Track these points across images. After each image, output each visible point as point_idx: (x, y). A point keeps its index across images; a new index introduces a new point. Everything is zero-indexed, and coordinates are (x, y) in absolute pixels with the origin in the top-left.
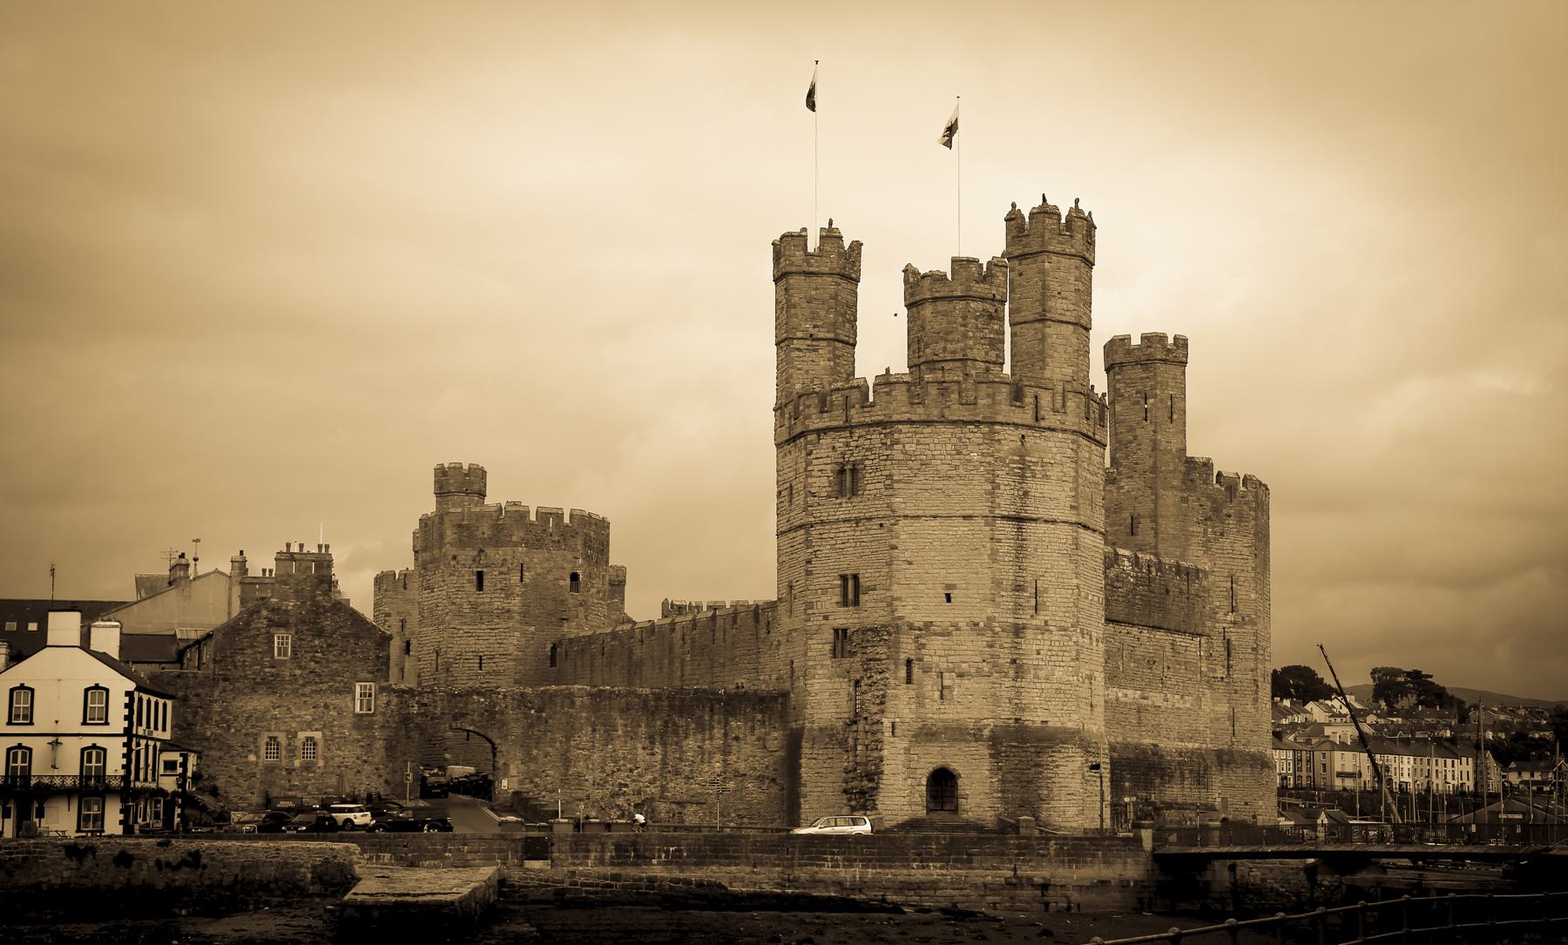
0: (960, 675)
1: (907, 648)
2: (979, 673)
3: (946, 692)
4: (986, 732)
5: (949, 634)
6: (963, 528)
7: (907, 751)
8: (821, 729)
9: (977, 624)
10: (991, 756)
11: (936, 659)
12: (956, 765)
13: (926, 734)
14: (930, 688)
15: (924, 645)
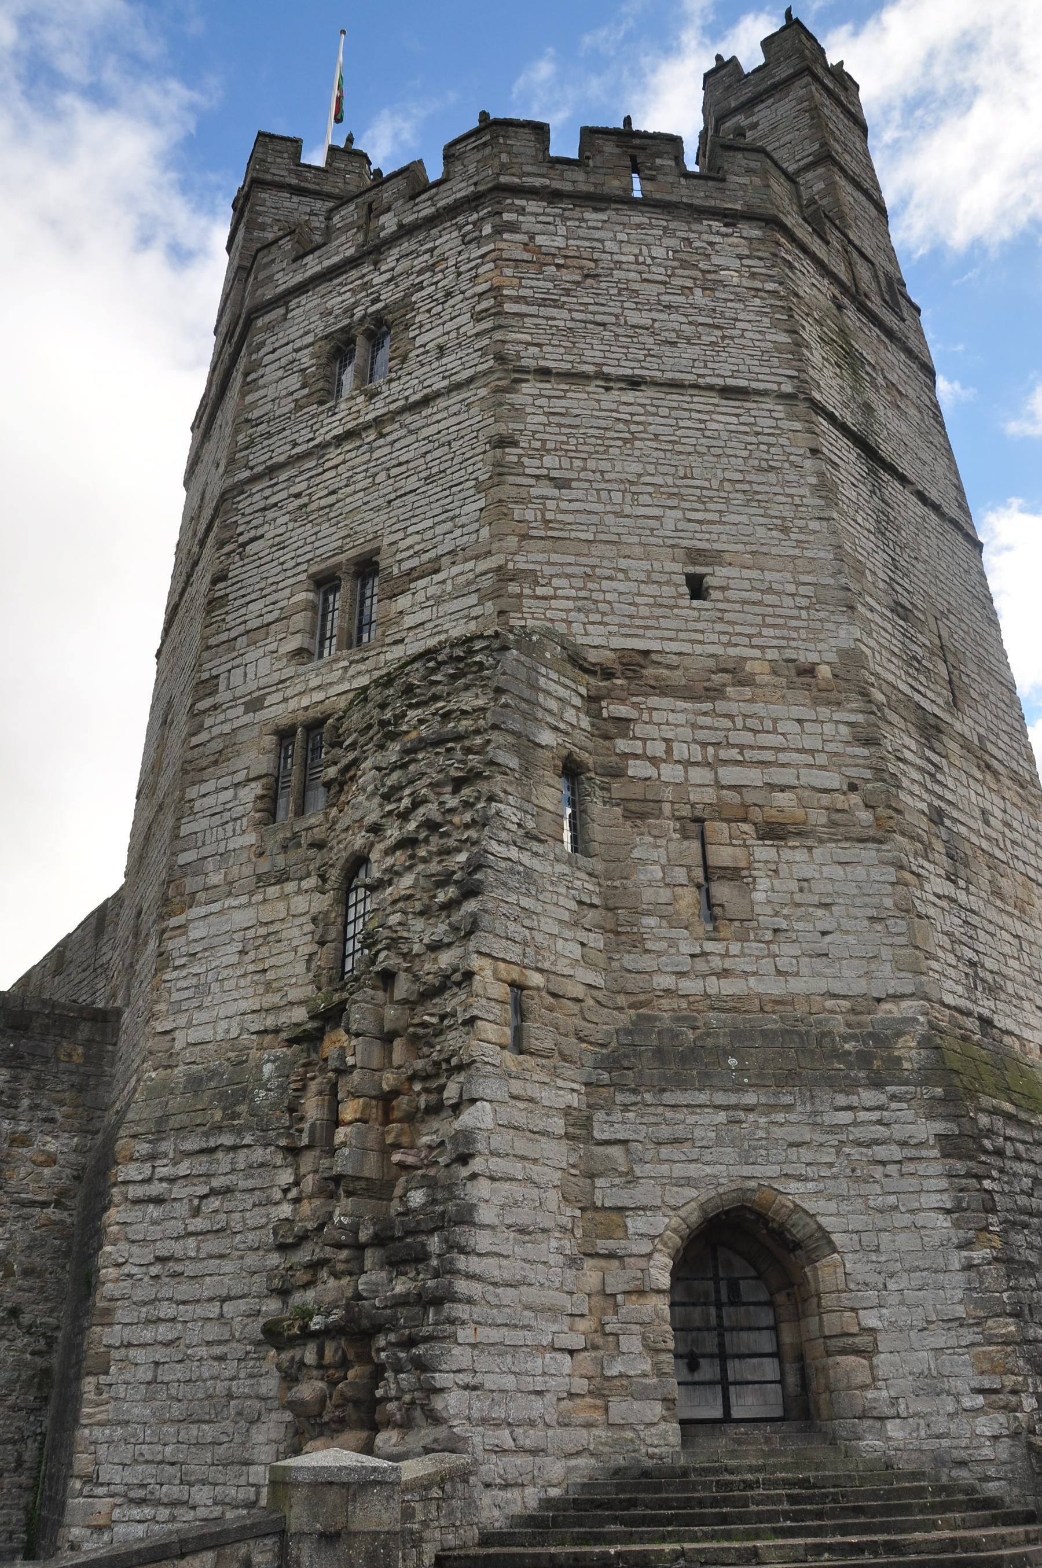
0: (774, 832)
1: (561, 712)
2: (840, 829)
3: (722, 891)
4: (909, 1051)
5: (714, 693)
6: (725, 417)
7: (579, 1128)
8: (195, 1083)
9: (808, 671)
10: (950, 1146)
11: (670, 772)
12: (809, 1191)
13: (651, 1056)
14: (658, 864)
15: (623, 723)
